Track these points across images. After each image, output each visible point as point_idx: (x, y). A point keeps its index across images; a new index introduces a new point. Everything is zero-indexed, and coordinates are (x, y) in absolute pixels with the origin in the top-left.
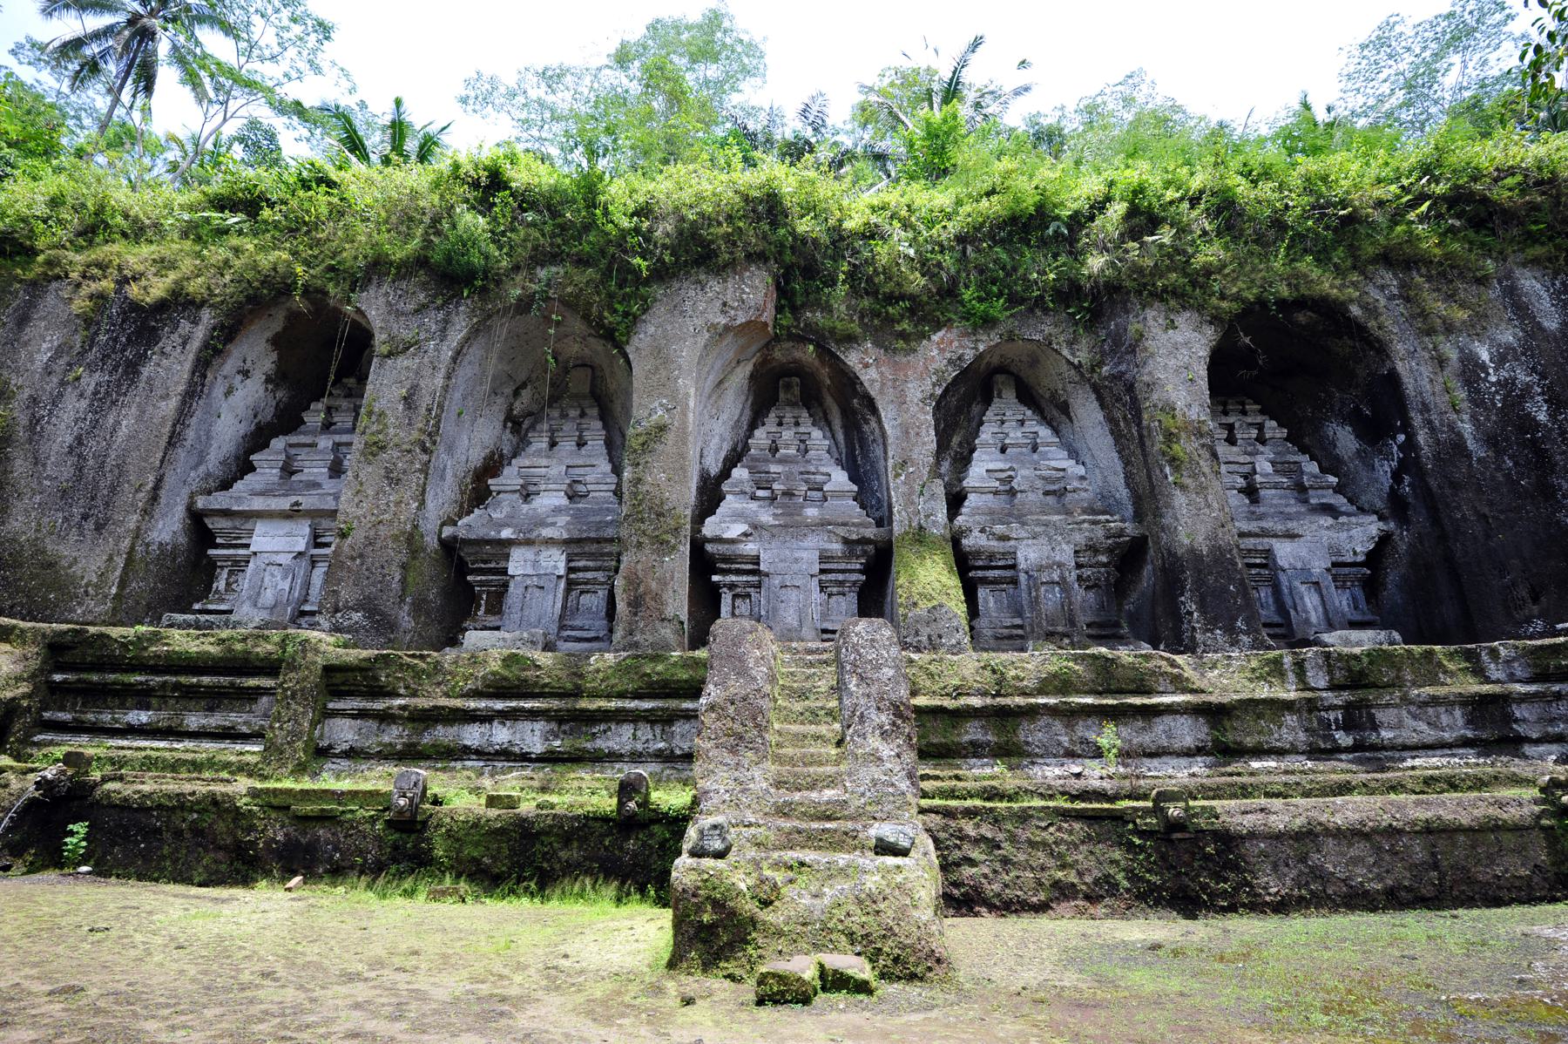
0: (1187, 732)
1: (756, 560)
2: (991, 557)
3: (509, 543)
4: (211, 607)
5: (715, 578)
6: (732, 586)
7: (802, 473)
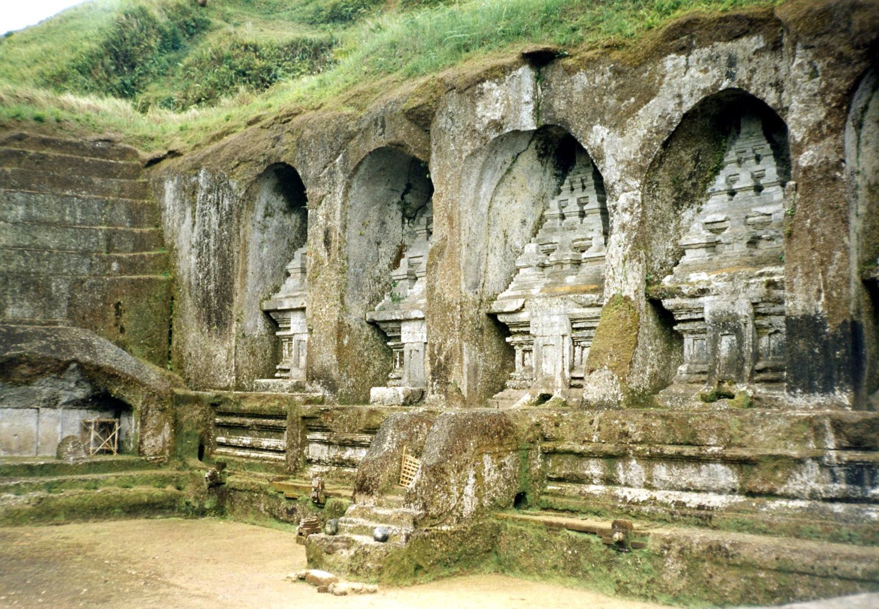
0: (726, 476)
2: (690, 311)
3: (398, 321)
4: (284, 367)
5: (508, 340)
6: (521, 344)
7: (573, 241)
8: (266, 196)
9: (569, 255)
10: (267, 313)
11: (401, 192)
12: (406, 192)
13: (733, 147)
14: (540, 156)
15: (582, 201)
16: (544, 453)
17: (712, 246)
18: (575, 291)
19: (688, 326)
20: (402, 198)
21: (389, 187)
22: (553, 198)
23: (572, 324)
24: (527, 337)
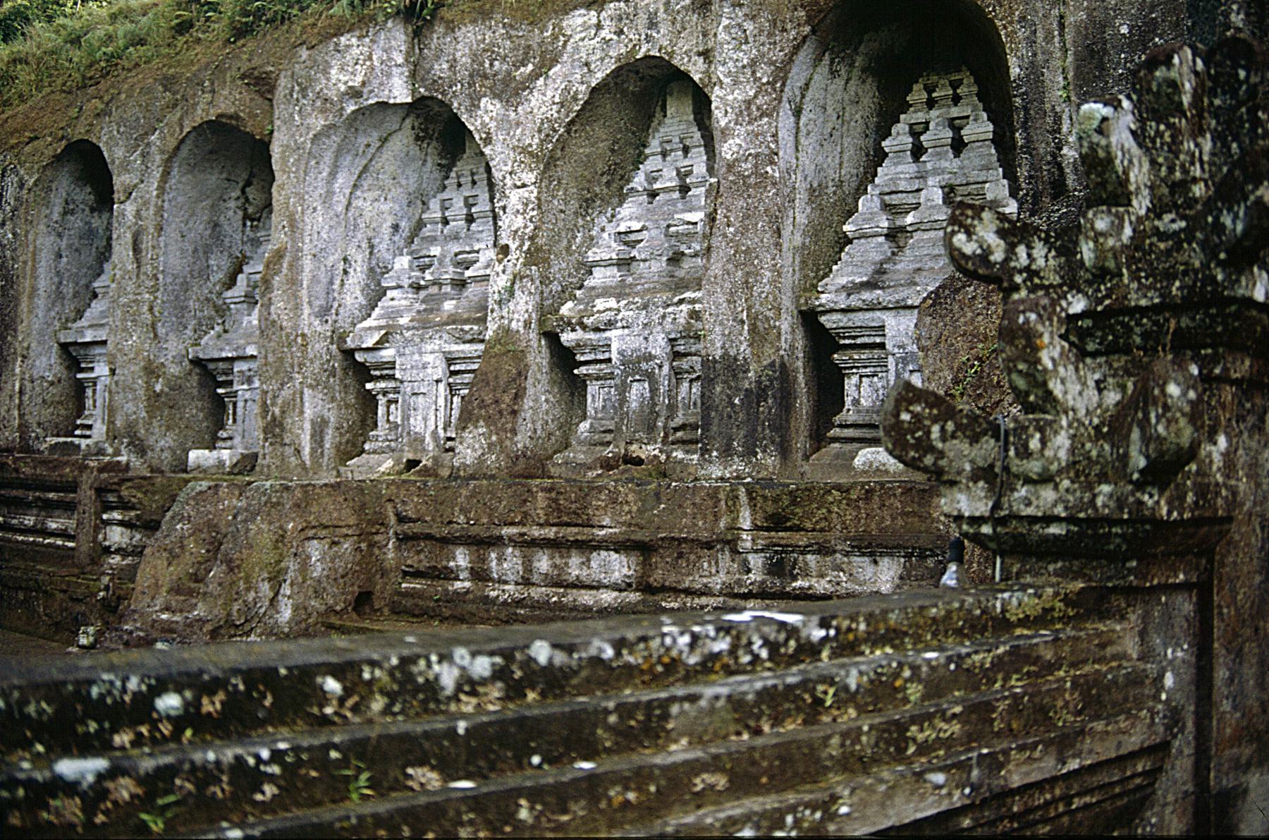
0: (619, 566)
1: (392, 366)
2: (594, 349)
3: (231, 360)
5: (369, 386)
6: (385, 393)
7: (456, 255)
8: (63, 186)
9: (449, 273)
10: (64, 347)
11: (241, 184)
12: (248, 183)
13: (657, 135)
14: (417, 138)
15: (471, 201)
16: (398, 539)
17: (625, 263)
18: (453, 319)
19: (591, 369)
20: (243, 192)
21: (224, 176)
22: (435, 197)
23: (450, 365)
24: (392, 384)
